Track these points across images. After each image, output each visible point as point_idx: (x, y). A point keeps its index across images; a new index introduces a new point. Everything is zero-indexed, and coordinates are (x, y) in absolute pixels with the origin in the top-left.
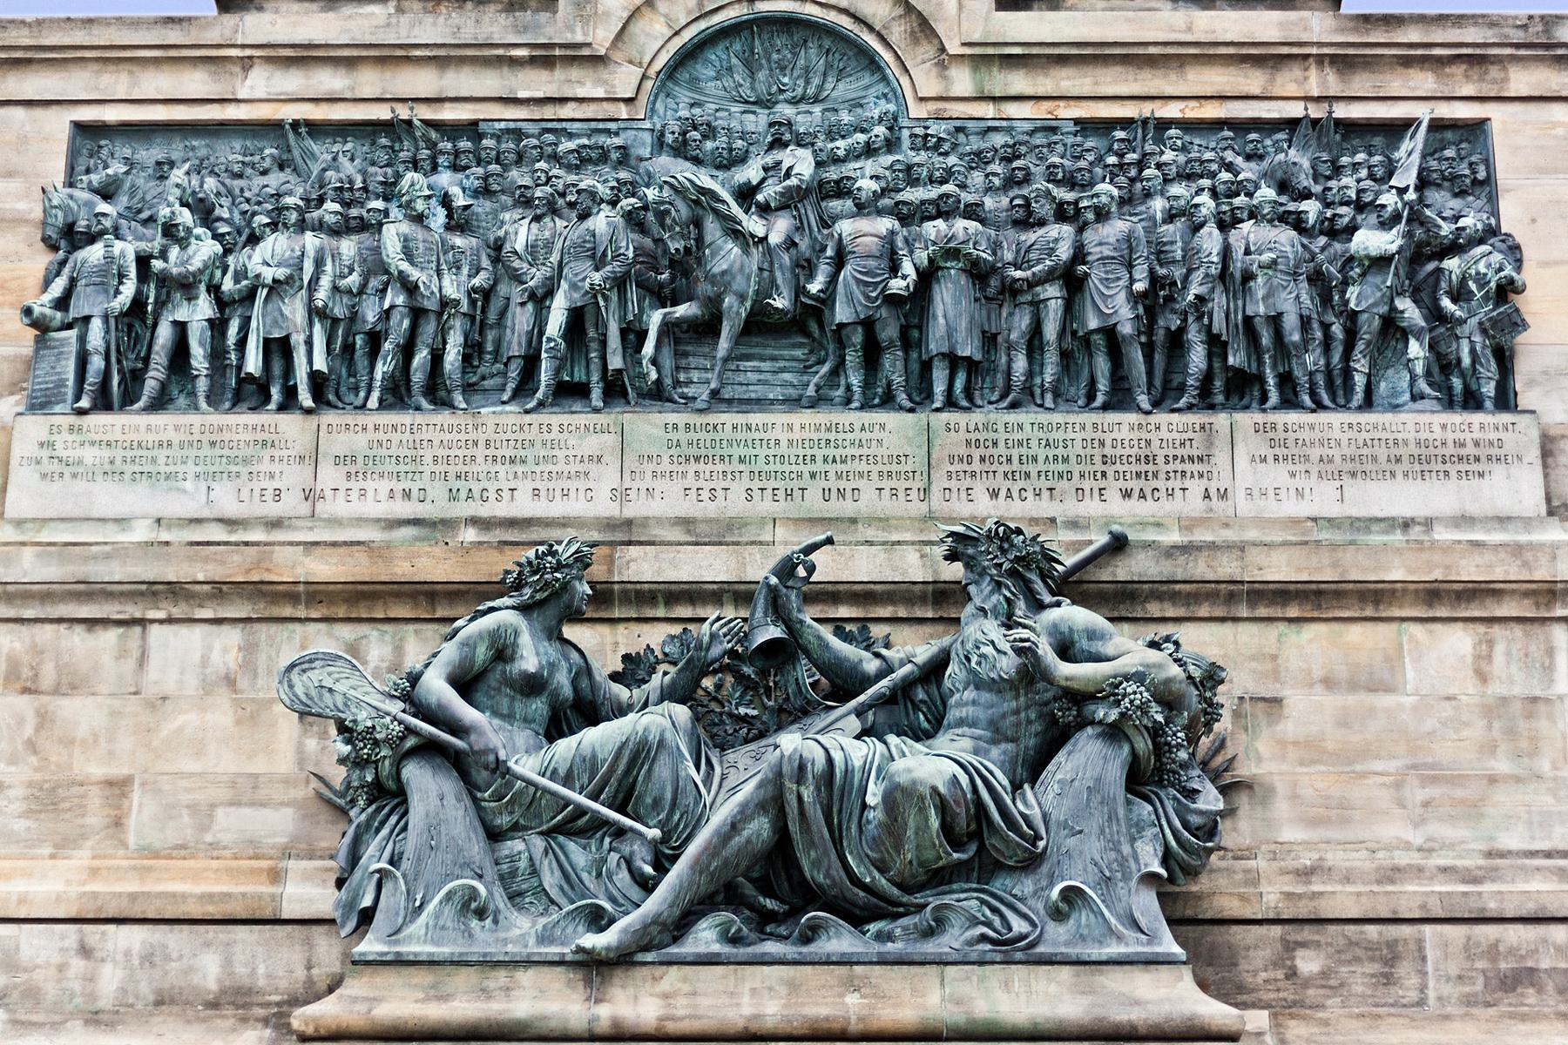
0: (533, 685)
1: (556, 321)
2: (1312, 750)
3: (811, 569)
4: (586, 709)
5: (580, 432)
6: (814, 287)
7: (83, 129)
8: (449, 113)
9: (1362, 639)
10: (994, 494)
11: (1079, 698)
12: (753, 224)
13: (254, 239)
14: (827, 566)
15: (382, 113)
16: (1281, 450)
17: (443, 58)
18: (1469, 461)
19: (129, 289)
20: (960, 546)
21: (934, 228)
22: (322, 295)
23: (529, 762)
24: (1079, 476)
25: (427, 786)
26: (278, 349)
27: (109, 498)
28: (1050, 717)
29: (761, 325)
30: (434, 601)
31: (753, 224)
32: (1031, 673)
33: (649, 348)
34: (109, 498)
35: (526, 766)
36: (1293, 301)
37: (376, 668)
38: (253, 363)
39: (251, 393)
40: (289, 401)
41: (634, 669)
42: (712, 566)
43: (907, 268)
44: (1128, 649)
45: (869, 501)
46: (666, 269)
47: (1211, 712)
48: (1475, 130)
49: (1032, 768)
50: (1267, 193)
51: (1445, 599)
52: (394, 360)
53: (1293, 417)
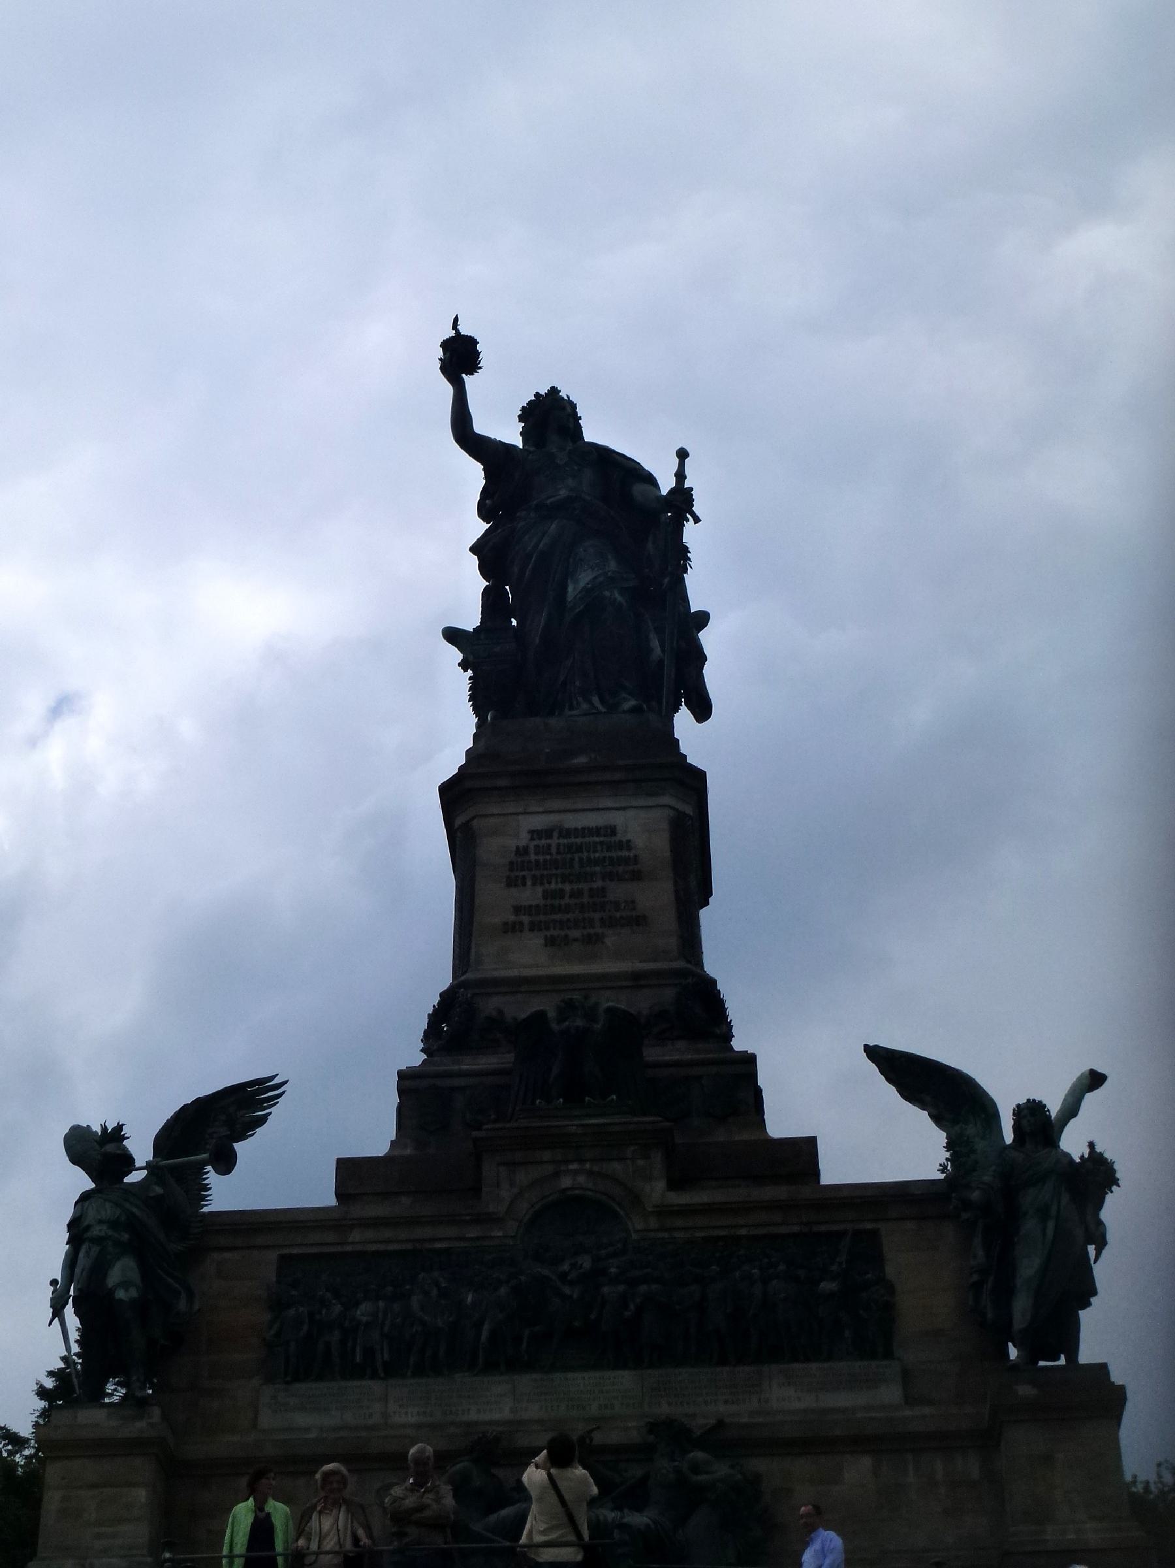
1: (483, 1338)
3: (591, 1440)
6: (593, 1317)
7: (282, 1258)
8: (438, 1245)
10: (670, 1404)
12: (567, 1290)
13: (357, 1304)
14: (598, 1438)
15: (409, 1246)
19: (305, 1328)
21: (643, 1288)
22: (386, 1329)
27: (302, 1419)
31: (567, 1290)
33: (524, 1345)
34: (302, 1419)
35: (477, 1527)
38: (358, 1359)
40: (374, 1376)
43: (632, 1307)
44: (722, 1470)
48: (874, 1235)
50: (782, 1267)
53: (796, 1366)
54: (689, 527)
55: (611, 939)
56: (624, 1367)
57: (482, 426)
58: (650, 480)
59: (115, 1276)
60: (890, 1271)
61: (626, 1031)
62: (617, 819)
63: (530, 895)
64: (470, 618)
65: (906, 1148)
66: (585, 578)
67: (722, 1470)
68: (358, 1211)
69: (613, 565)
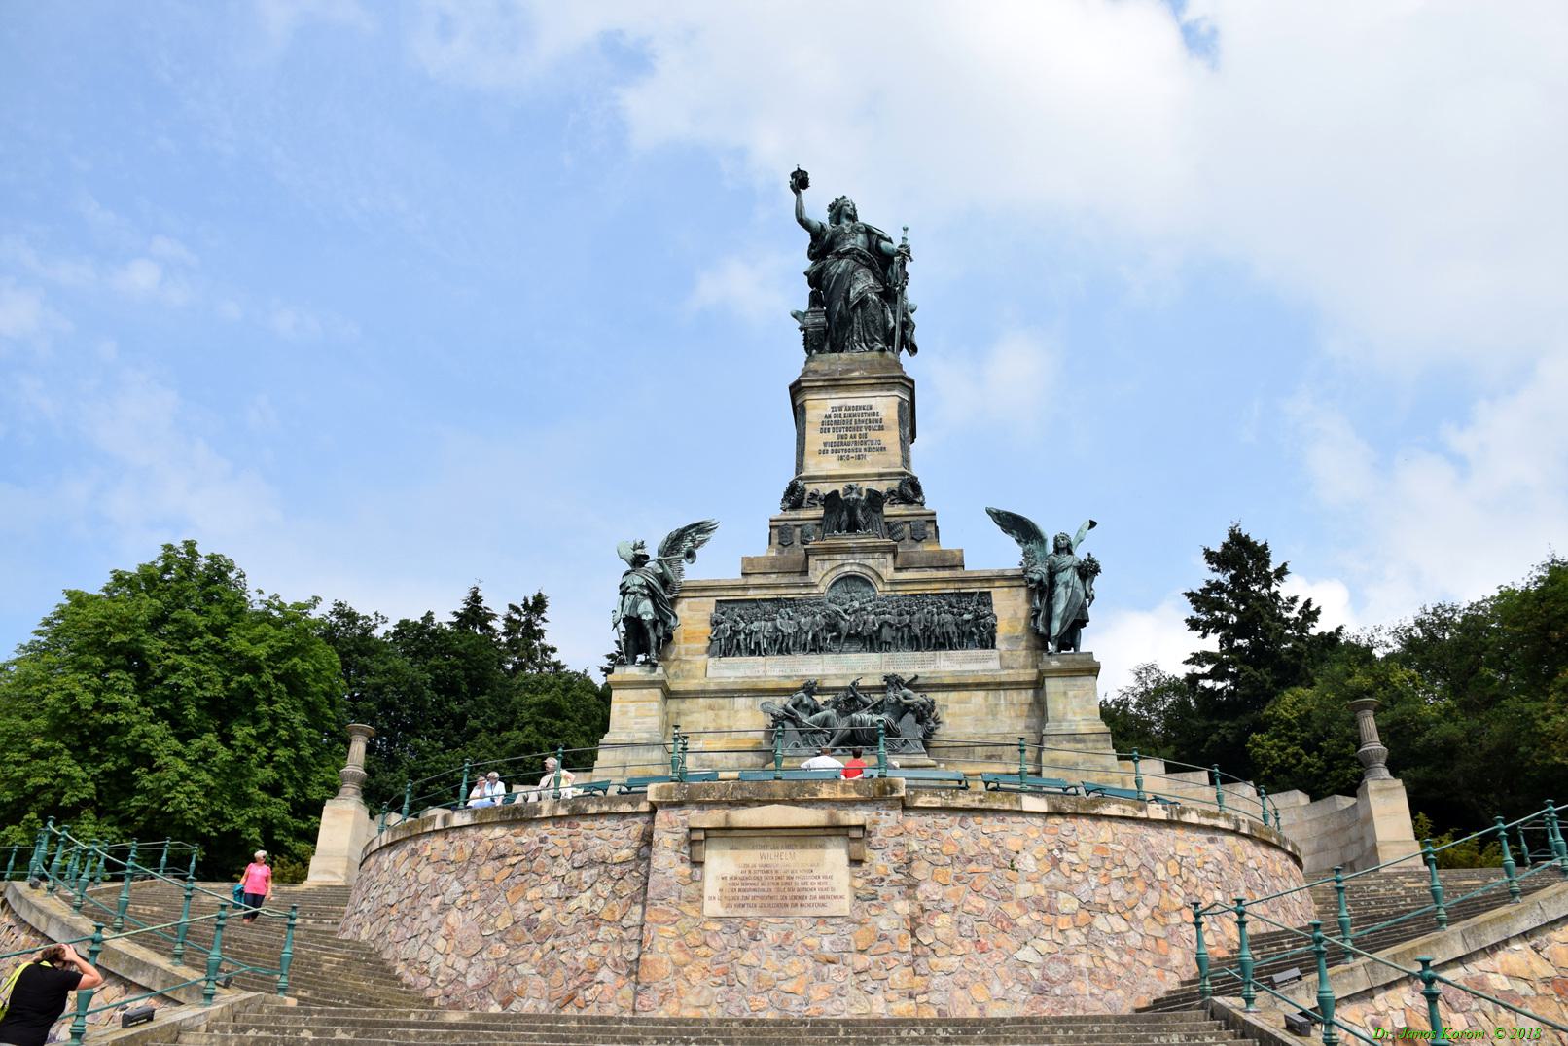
0: (807, 706)
2: (954, 715)
4: (817, 710)
5: (814, 658)
9: (964, 694)
11: (907, 706)
14: (861, 683)
16: (949, 659)
17: (787, 586)
18: (986, 660)
20: (886, 678)
23: (806, 719)
24: (908, 664)
25: (789, 726)
26: (757, 644)
27: (727, 673)
28: (901, 710)
29: (850, 637)
30: (787, 692)
32: (898, 701)
34: (727, 673)
36: (952, 629)
37: (779, 703)
39: (752, 653)
41: (826, 703)
42: (840, 683)
45: (870, 670)
46: (832, 626)
47: (932, 709)
49: (899, 719)
51: (979, 686)
52: (781, 645)
54: (908, 263)
55: (870, 457)
56: (873, 650)
57: (808, 215)
58: (890, 241)
59: (641, 609)
60: (995, 610)
61: (875, 500)
62: (872, 401)
63: (832, 437)
64: (804, 306)
65: (1008, 554)
66: (859, 287)
67: (917, 697)
68: (753, 580)
69: (871, 281)
